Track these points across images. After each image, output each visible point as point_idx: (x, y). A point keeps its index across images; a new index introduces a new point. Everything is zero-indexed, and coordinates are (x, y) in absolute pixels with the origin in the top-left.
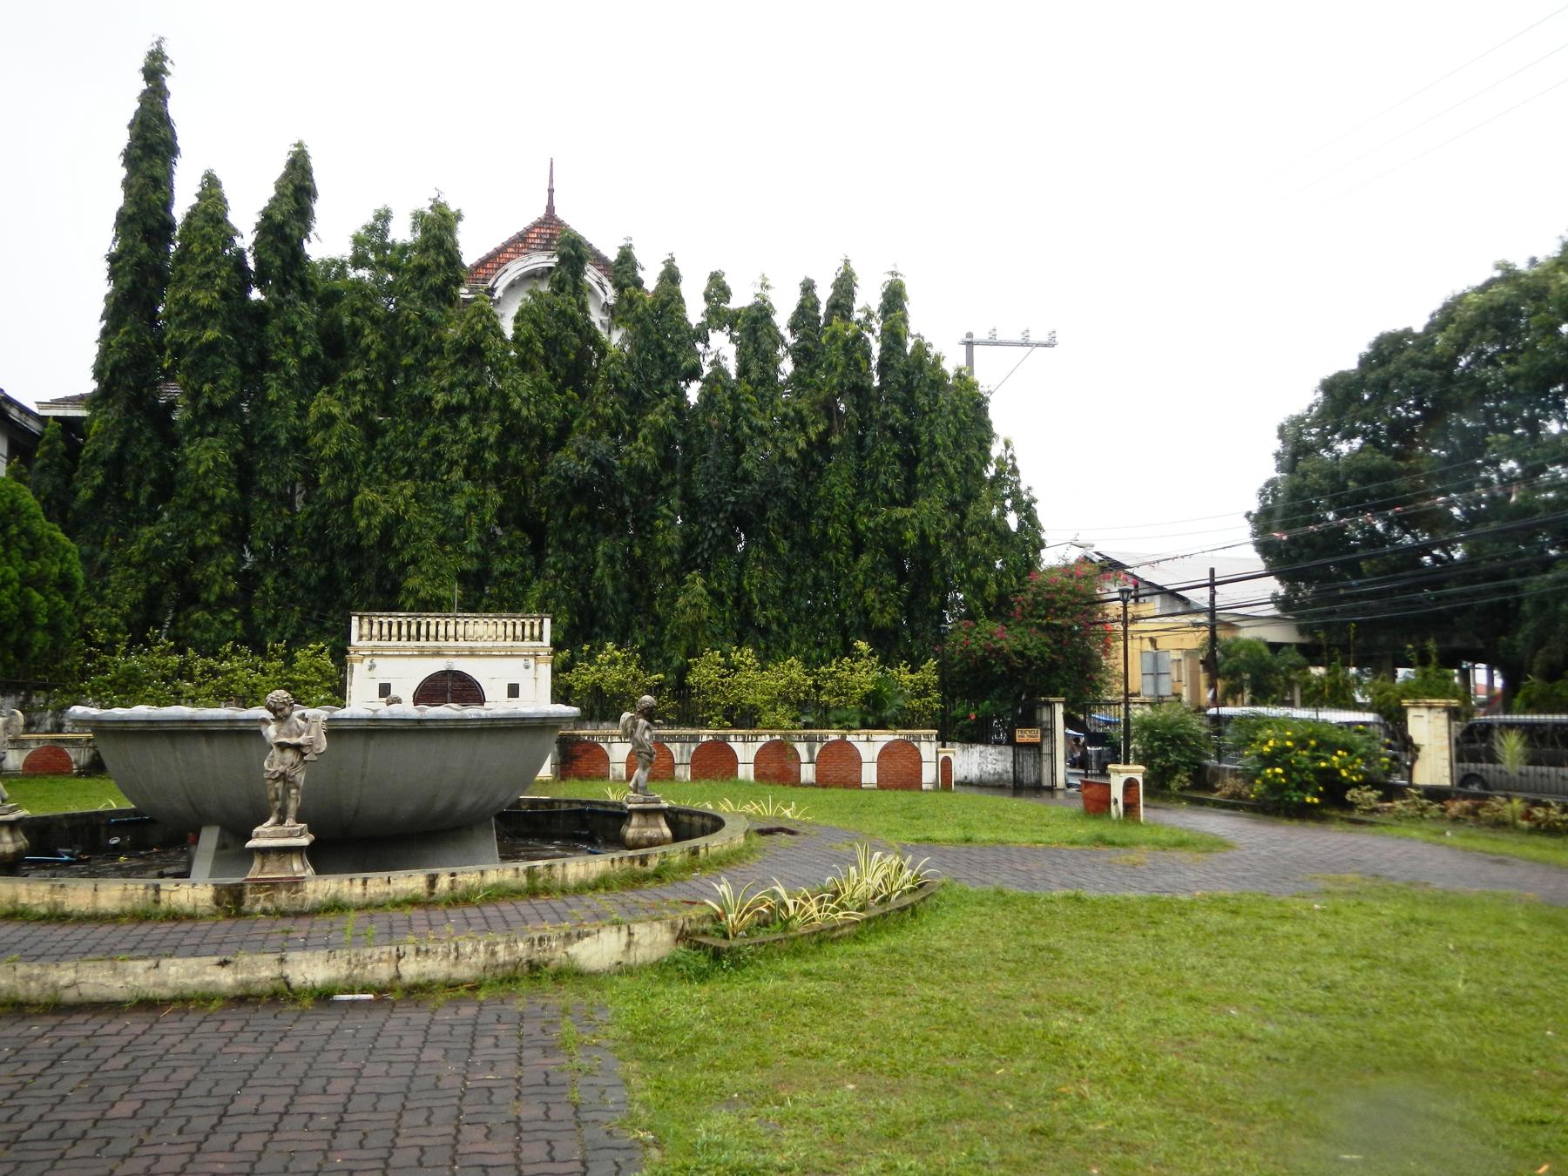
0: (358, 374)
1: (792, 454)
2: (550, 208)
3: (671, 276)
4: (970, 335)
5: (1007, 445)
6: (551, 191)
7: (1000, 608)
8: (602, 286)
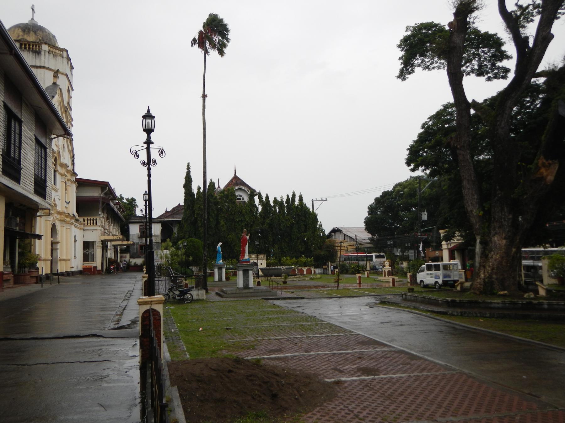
0: (223, 215)
1: (288, 225)
2: (235, 174)
3: (267, 197)
4: (313, 200)
5: (320, 222)
6: (235, 171)
7: (320, 248)
8: (248, 191)
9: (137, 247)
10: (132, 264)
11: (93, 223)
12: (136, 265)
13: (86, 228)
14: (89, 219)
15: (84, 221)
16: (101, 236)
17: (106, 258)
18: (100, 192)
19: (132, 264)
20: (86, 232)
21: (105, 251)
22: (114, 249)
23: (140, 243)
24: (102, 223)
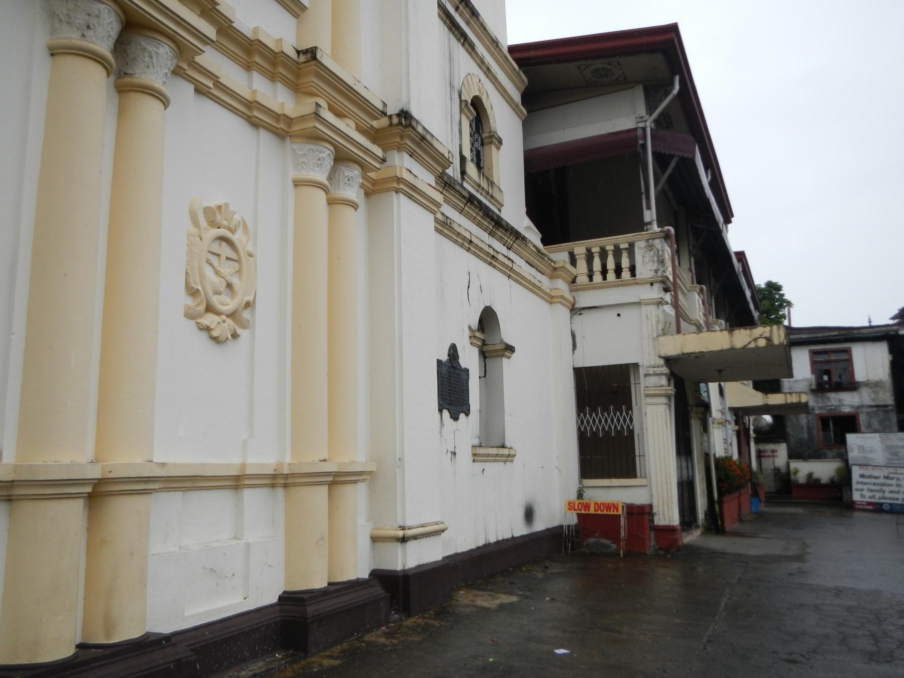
9: (808, 421)
10: (801, 477)
11: (618, 271)
12: (813, 483)
13: (585, 299)
14: (595, 250)
15: (573, 261)
16: (664, 333)
17: (707, 456)
18: (642, 110)
19: (801, 477)
20: (588, 318)
21: (695, 426)
22: (737, 423)
23: (820, 408)
24: (662, 262)
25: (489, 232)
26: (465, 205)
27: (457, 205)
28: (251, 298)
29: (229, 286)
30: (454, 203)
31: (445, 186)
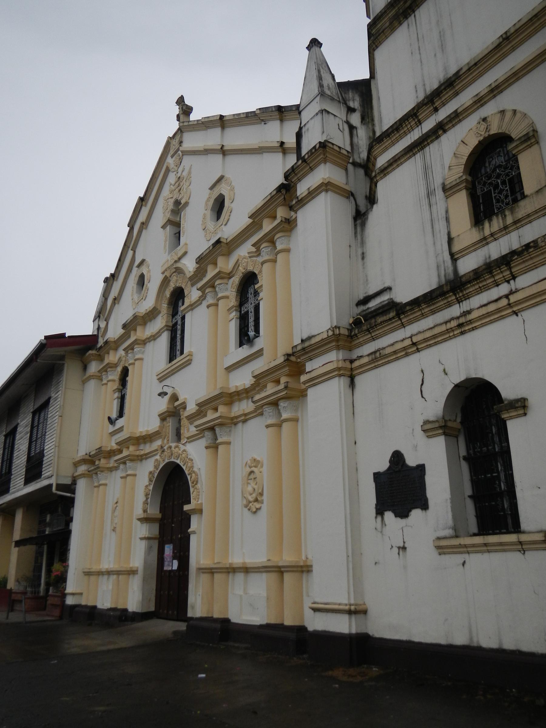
25: (457, 302)
26: (401, 320)
27: (384, 332)
28: (260, 491)
29: (254, 489)
30: (383, 333)
31: (369, 331)
